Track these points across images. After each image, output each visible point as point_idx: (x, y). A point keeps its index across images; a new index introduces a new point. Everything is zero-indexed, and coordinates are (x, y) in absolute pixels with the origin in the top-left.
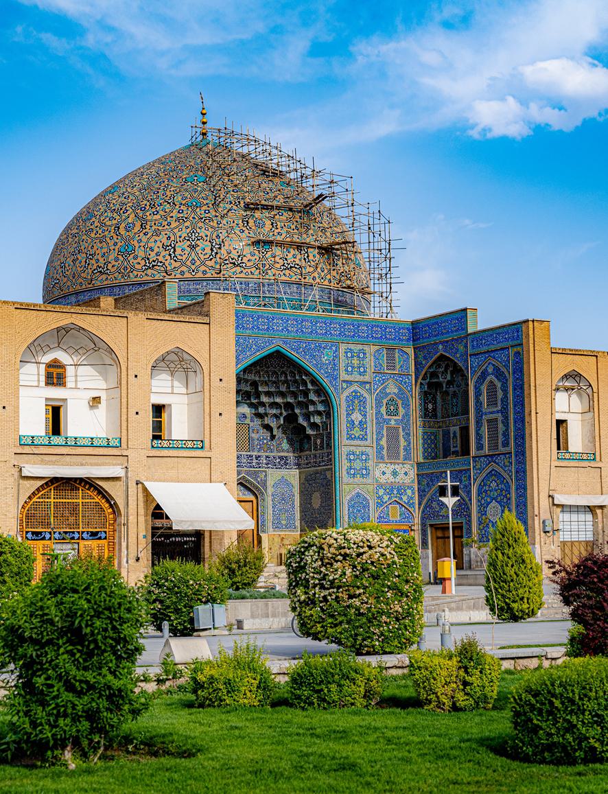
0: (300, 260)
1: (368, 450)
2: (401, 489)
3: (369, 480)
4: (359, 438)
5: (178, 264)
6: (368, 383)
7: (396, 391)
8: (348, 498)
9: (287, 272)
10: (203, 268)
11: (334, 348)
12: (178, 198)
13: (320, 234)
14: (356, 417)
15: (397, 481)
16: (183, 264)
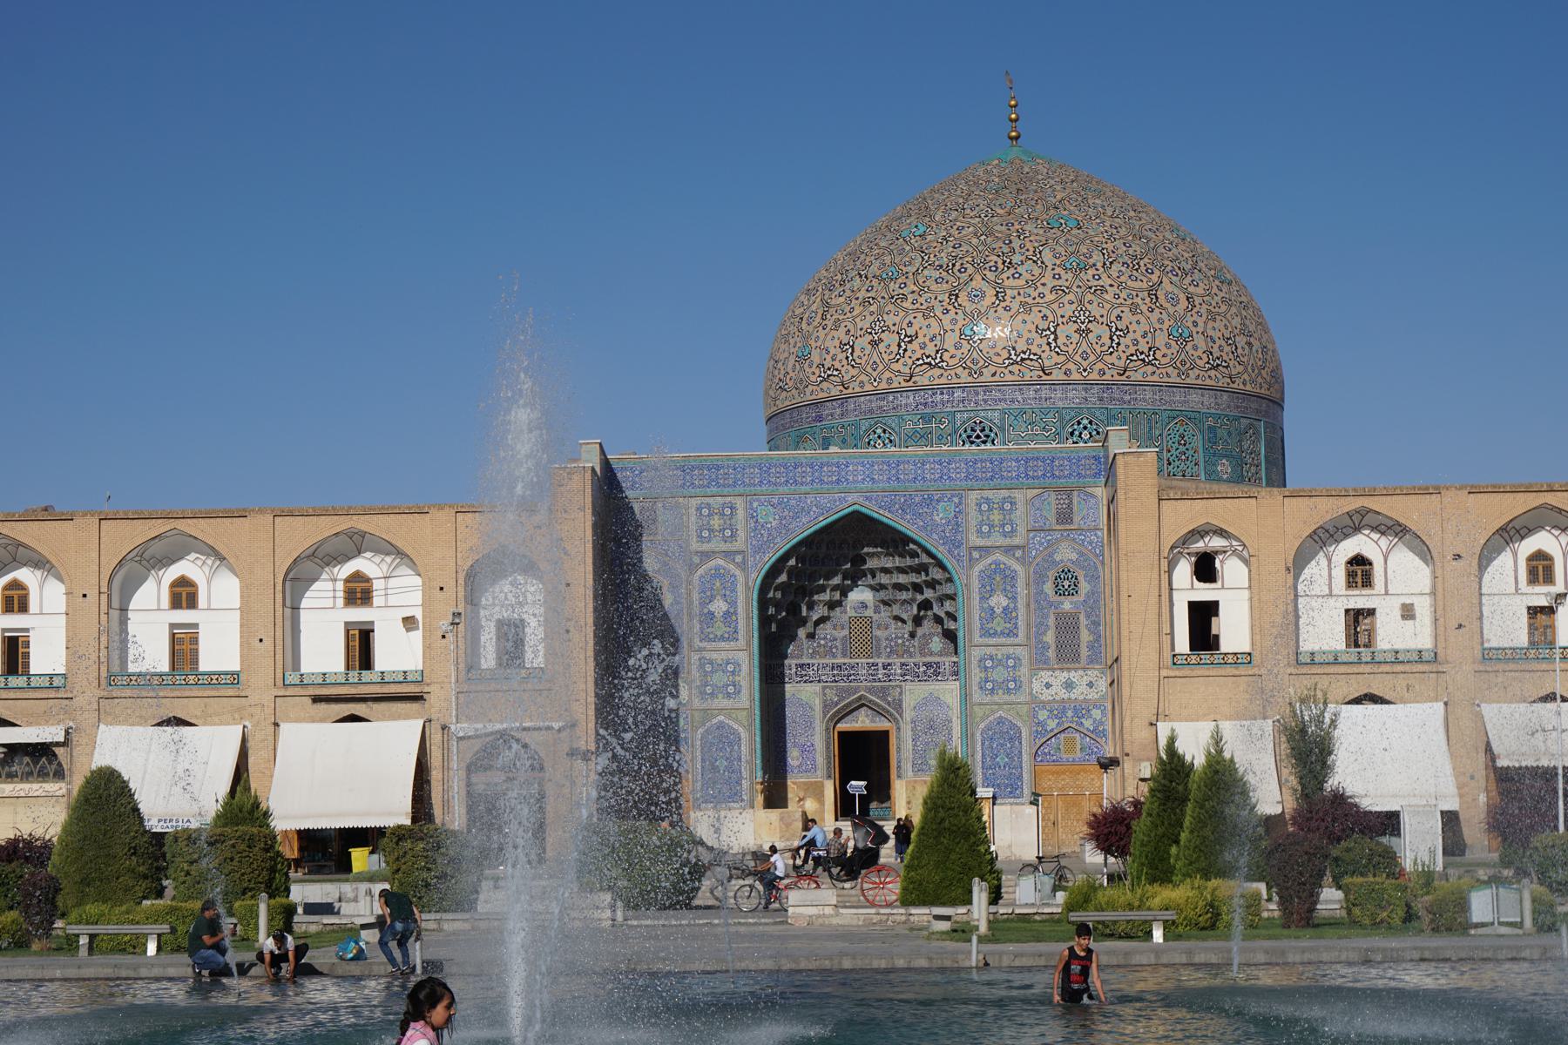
0: (1040, 346)
1: (1019, 650)
2: (1081, 710)
3: (1022, 697)
4: (1002, 633)
5: (854, 372)
6: (1018, 547)
7: (1074, 556)
8: (982, 726)
9: (1015, 368)
10: (887, 374)
11: (956, 500)
12: (874, 269)
13: (1089, 297)
14: (999, 601)
15: (1073, 696)
16: (863, 371)
